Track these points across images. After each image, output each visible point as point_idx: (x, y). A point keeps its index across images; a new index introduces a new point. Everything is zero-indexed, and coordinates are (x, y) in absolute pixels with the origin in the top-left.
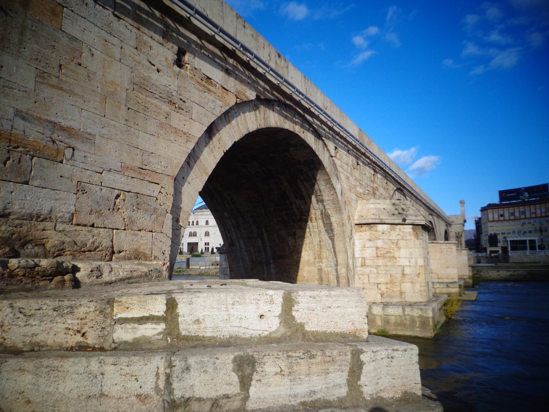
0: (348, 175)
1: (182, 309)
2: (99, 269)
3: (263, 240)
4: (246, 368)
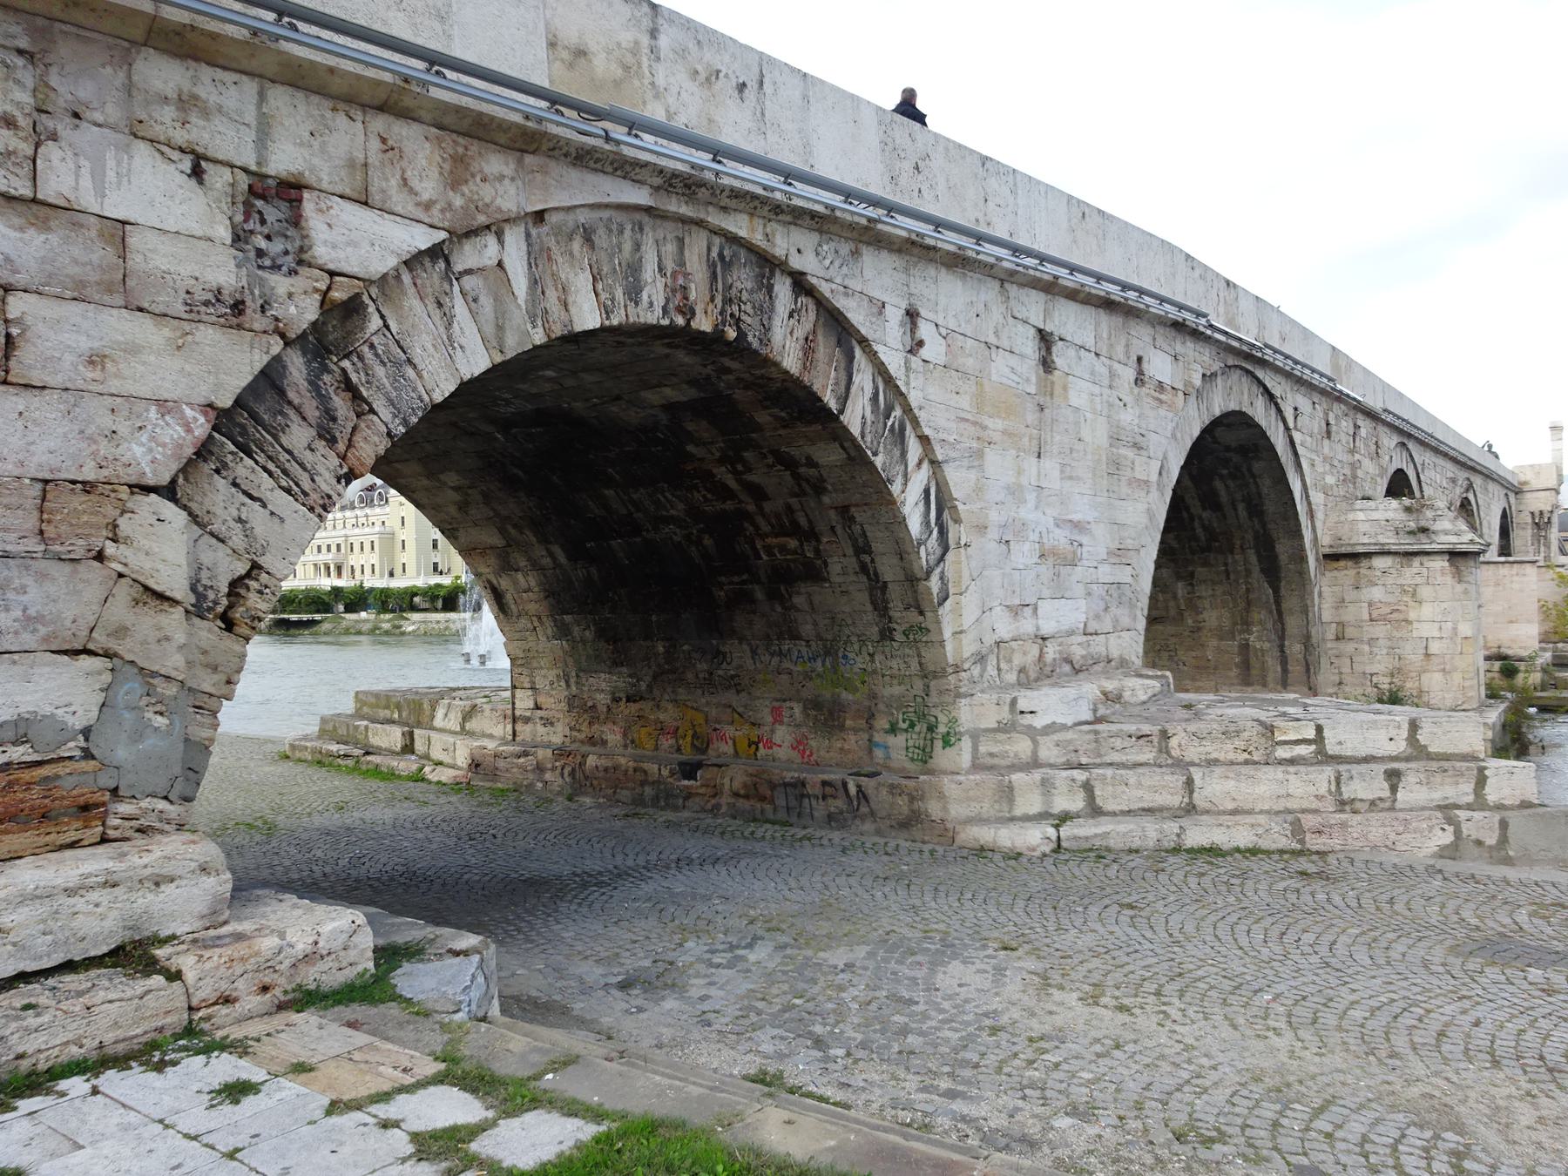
1: (1326, 733)
4: (1393, 777)
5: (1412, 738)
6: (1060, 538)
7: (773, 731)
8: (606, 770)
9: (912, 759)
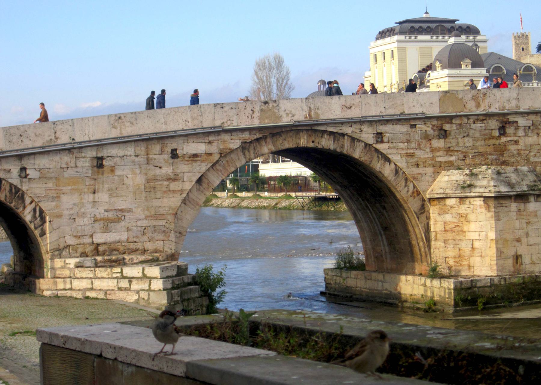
0: (412, 151)
1: (124, 271)
2: (132, 259)
3: (371, 212)
4: (130, 282)
5: (143, 273)
6: (110, 215)
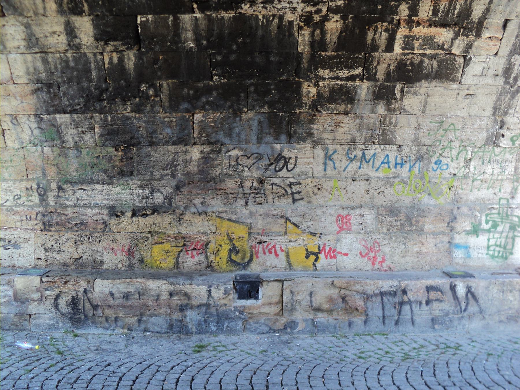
7: (338, 240)
8: (126, 296)
9: (493, 257)
